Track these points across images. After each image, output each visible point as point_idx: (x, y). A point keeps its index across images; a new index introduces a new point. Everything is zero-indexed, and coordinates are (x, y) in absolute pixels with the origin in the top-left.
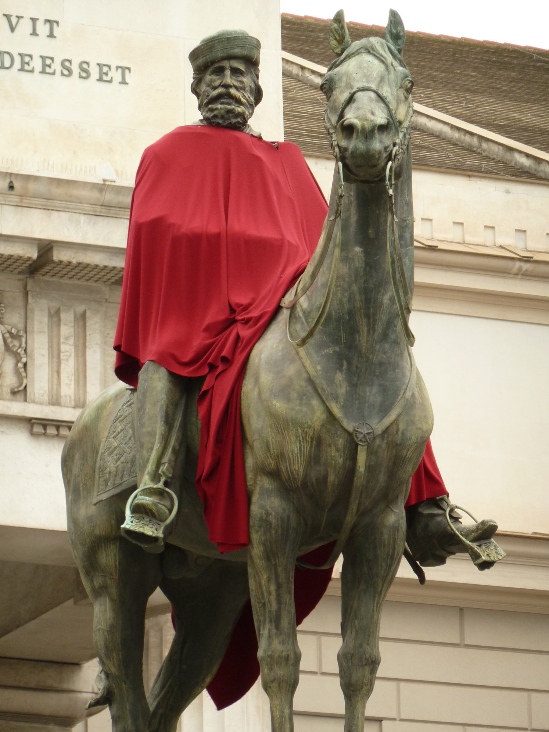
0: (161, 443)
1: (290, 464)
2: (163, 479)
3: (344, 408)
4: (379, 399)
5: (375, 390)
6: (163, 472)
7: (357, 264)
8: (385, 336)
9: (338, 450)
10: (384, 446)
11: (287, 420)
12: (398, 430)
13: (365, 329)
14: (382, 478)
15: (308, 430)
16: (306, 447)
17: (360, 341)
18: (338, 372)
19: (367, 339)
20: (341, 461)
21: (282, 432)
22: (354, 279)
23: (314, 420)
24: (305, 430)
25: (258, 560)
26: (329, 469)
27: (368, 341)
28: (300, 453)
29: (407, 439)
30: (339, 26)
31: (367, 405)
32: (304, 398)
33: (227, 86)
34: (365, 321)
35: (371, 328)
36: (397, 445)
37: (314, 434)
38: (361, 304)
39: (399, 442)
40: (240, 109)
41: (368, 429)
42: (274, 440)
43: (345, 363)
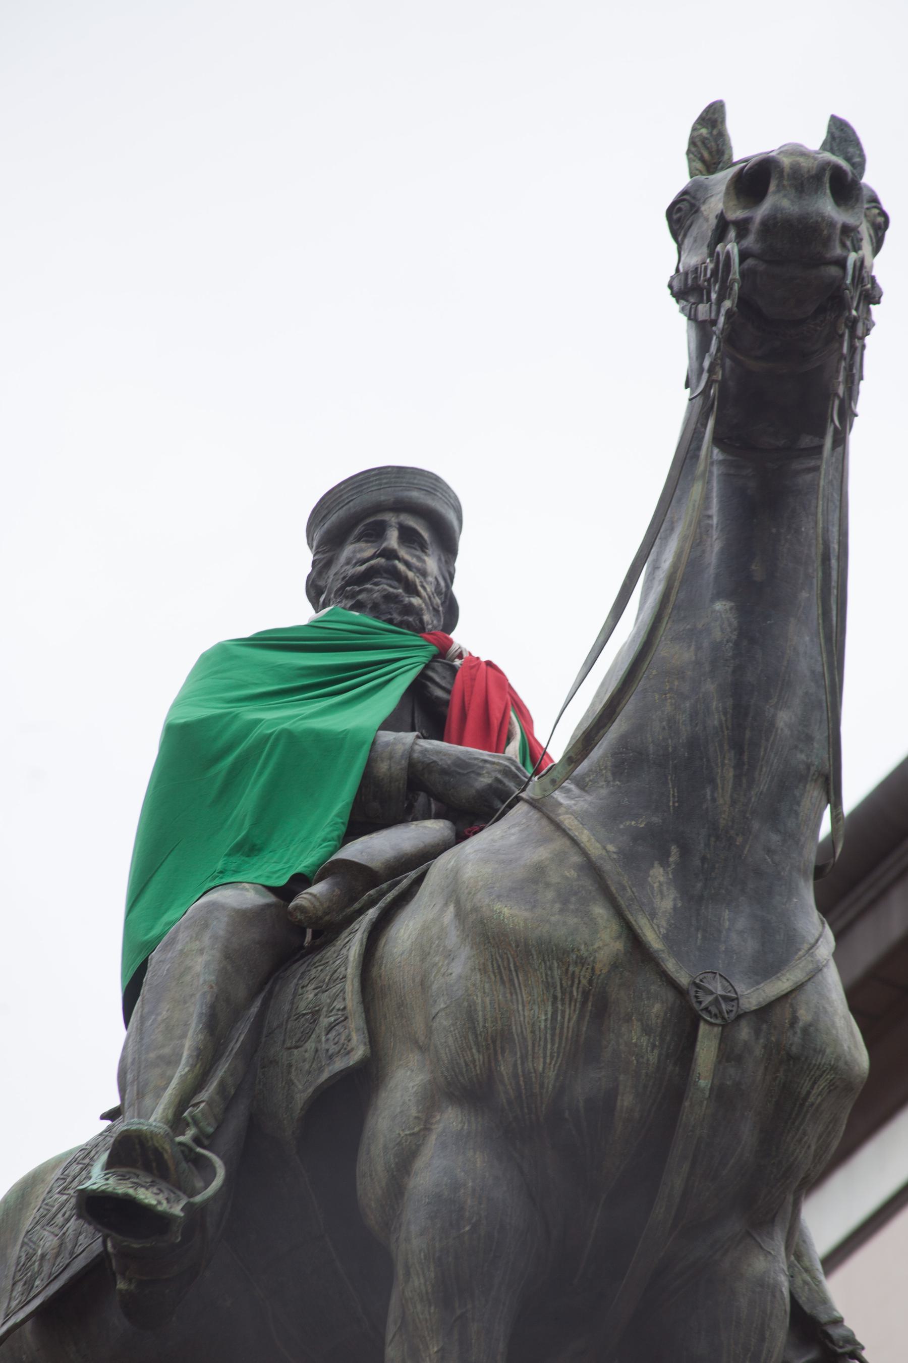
0: (193, 1066)
1: (524, 1058)
2: (191, 1132)
3: (666, 938)
4: (751, 946)
5: (741, 923)
6: (193, 1118)
7: (717, 635)
8: (773, 817)
9: (647, 1030)
10: (758, 1051)
11: (526, 944)
12: (794, 1020)
13: (730, 774)
14: (747, 1132)
15: (577, 970)
16: (570, 1015)
17: (714, 800)
18: (656, 864)
19: (731, 796)
20: (653, 1057)
21: (511, 980)
22: (707, 668)
23: (595, 946)
24: (571, 969)
25: (419, 1307)
26: (622, 1077)
27: (734, 802)
28: (553, 1029)
29: (815, 1050)
30: (711, 133)
31: (722, 948)
32: (573, 899)
33: (390, 554)
35: (745, 770)
36: (791, 1058)
37: (590, 982)
38: (723, 718)
39: (794, 1049)
40: (416, 601)
41: (724, 988)
42: (488, 1000)
43: (674, 849)
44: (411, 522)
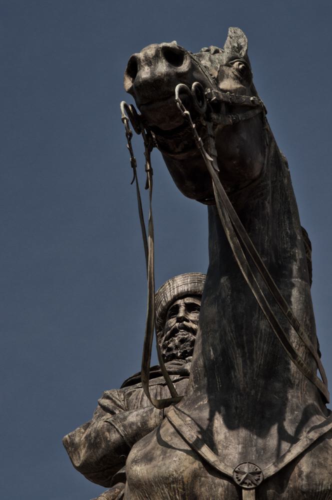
11: (149, 482)
13: (240, 361)
17: (235, 377)
19: (243, 372)
23: (181, 471)
24: (172, 486)
27: (245, 375)
29: (316, 484)
33: (180, 320)
34: (238, 351)
36: (303, 493)
38: (232, 335)
39: (304, 488)
44: (189, 300)
